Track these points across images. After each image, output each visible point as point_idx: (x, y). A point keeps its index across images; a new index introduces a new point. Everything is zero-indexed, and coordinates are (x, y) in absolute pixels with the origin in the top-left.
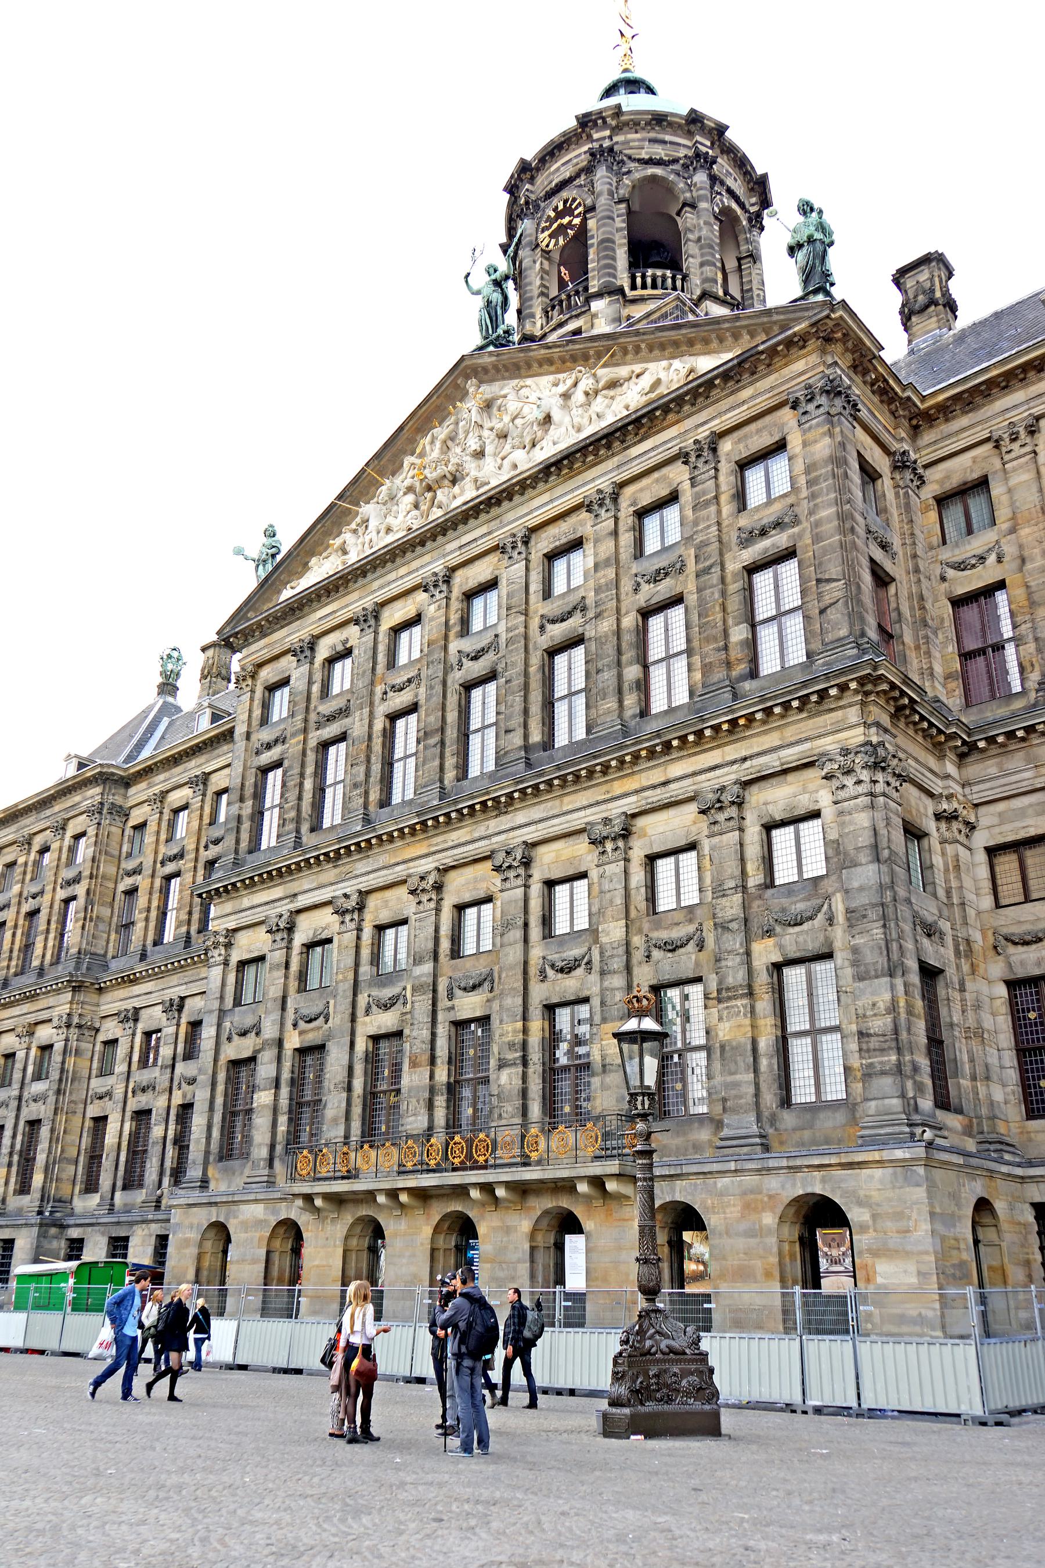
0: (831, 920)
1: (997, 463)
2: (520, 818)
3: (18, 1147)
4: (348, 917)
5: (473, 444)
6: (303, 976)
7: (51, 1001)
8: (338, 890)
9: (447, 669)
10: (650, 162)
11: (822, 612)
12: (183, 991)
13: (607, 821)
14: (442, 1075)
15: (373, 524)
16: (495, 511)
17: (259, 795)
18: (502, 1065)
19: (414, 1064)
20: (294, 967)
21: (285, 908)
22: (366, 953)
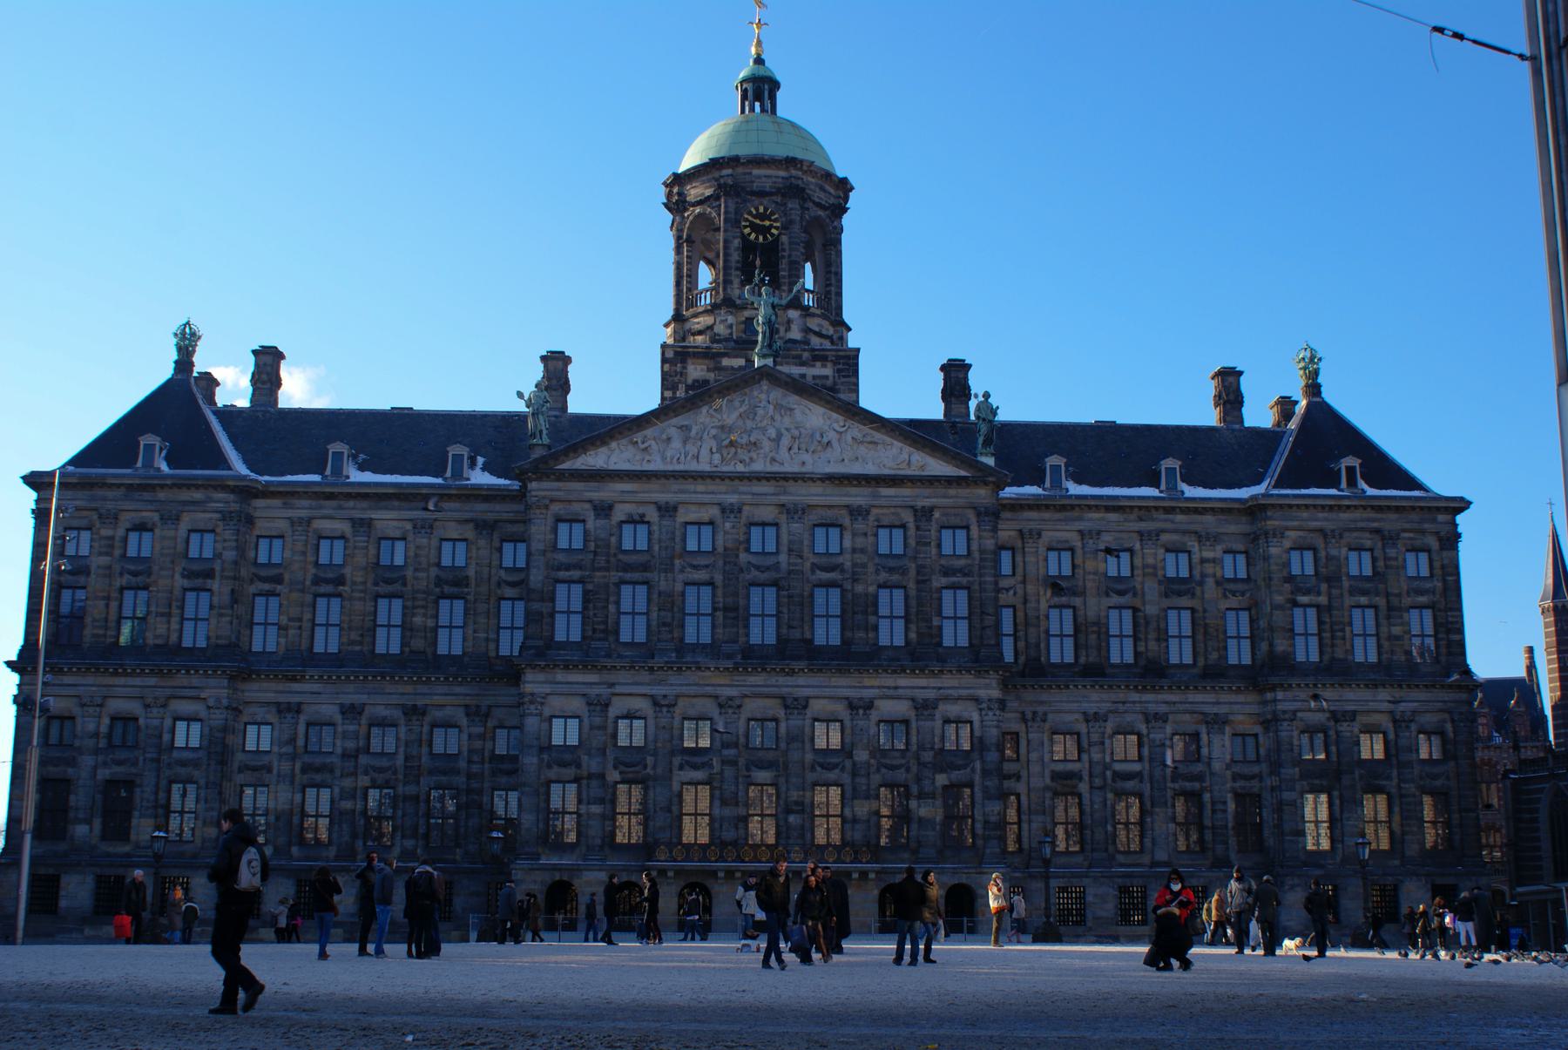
0: (973, 770)
1: (1019, 544)
2: (801, 681)
6: (615, 736)
7: (195, 681)
8: (658, 691)
9: (742, 570)
10: (819, 205)
12: (363, 698)
15: (676, 444)
16: (782, 483)
17: (553, 600)
18: (788, 811)
19: (724, 803)
20: (610, 730)
21: (603, 691)
22: (676, 732)
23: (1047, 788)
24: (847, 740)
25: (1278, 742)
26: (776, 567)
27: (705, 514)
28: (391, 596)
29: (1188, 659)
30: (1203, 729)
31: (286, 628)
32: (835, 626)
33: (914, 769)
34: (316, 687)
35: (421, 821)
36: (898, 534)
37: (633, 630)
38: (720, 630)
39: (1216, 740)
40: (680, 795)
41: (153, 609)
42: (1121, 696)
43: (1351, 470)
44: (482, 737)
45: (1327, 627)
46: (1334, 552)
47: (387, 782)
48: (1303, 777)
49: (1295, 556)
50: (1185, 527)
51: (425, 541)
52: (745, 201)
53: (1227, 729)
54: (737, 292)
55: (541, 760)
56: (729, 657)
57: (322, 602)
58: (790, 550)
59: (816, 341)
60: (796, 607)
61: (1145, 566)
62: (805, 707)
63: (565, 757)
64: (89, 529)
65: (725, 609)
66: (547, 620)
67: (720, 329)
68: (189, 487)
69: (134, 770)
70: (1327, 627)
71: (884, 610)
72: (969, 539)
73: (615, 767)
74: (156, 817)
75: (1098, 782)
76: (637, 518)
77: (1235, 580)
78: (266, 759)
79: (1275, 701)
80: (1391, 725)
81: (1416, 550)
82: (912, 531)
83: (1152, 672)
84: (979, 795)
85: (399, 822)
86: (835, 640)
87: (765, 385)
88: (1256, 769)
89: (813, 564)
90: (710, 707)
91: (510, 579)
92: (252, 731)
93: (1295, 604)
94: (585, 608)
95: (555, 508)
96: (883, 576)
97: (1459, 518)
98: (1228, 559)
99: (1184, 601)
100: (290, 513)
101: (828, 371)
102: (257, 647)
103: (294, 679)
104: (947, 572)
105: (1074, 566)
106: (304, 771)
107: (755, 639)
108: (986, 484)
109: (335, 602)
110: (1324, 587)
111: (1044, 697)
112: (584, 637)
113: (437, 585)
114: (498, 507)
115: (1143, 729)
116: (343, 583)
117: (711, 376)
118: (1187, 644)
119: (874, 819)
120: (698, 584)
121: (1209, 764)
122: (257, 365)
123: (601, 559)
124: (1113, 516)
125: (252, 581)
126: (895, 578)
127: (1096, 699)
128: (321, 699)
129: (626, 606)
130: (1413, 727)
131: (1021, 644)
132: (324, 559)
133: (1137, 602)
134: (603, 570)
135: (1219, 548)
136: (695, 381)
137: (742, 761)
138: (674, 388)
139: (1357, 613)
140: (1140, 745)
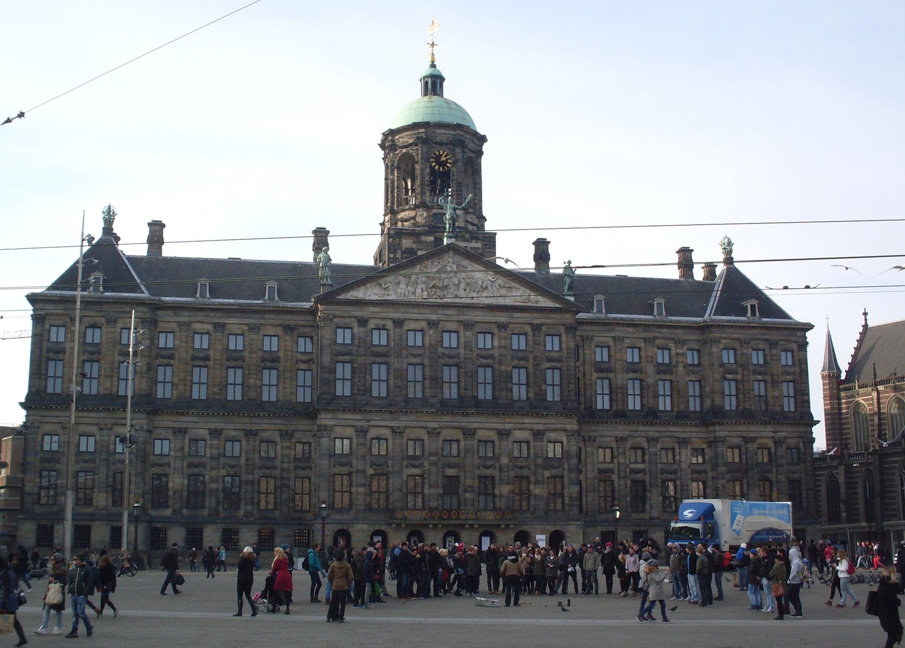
0: (564, 469)
2: (472, 419)
3: (111, 483)
5: (455, 281)
8: (395, 424)
10: (472, 151)
12: (219, 426)
14: (441, 491)
15: (403, 286)
16: (461, 309)
17: (335, 372)
18: (466, 491)
19: (431, 486)
20: (368, 445)
21: (364, 424)
22: (405, 447)
23: (596, 478)
24: (497, 451)
25: (716, 453)
27: (417, 325)
28: (235, 367)
29: (668, 408)
30: (677, 446)
31: (177, 385)
32: (489, 388)
33: (533, 467)
35: (256, 495)
36: (523, 338)
37: (379, 390)
38: (428, 391)
39: (683, 452)
40: (407, 482)
41: (102, 373)
42: (634, 428)
43: (753, 307)
44: (289, 448)
45: (741, 391)
46: (745, 351)
47: (236, 473)
48: (729, 471)
49: (725, 352)
50: (668, 336)
51: (255, 336)
52: (432, 147)
53: (689, 446)
54: (428, 199)
55: (330, 462)
56: (432, 406)
57: (196, 370)
59: (470, 227)
60: (469, 378)
61: (647, 357)
62: (474, 434)
63: (343, 460)
64: (64, 326)
65: (431, 379)
67: (419, 220)
68: (122, 303)
69: (93, 465)
70: (741, 391)
71: (515, 380)
72: (560, 342)
74: (107, 492)
75: (622, 474)
77: (693, 365)
78: (166, 459)
79: (715, 431)
80: (772, 445)
81: (785, 351)
82: (530, 337)
83: (650, 415)
84: (566, 483)
85: (243, 495)
86: (489, 396)
87: (451, 253)
88: (703, 468)
89: (478, 355)
90: (423, 434)
91: (304, 358)
92: (158, 443)
93: (726, 379)
94: (353, 377)
95: (336, 320)
96: (515, 362)
97: (808, 334)
98: (689, 353)
99: (668, 377)
100: (178, 319)
101: (479, 245)
102: (160, 395)
103: (183, 414)
104: (549, 360)
105: (609, 356)
106: (189, 466)
107: (446, 396)
108: (570, 311)
109: (204, 370)
110: (740, 370)
111: (594, 428)
112: (352, 394)
114: (296, 317)
115: (645, 445)
116: (209, 360)
117: (415, 246)
118: (668, 400)
119: (511, 495)
120: (414, 365)
121: (680, 465)
122: (151, 232)
123: (362, 350)
124: (630, 329)
125: (157, 358)
126: (522, 363)
127: (621, 430)
128: (199, 427)
129: (375, 376)
130: (784, 445)
131: (582, 399)
132: (197, 345)
133: (642, 377)
134: (362, 356)
135: (685, 347)
137: (440, 464)
138: (395, 253)
139: (756, 384)
140: (644, 454)
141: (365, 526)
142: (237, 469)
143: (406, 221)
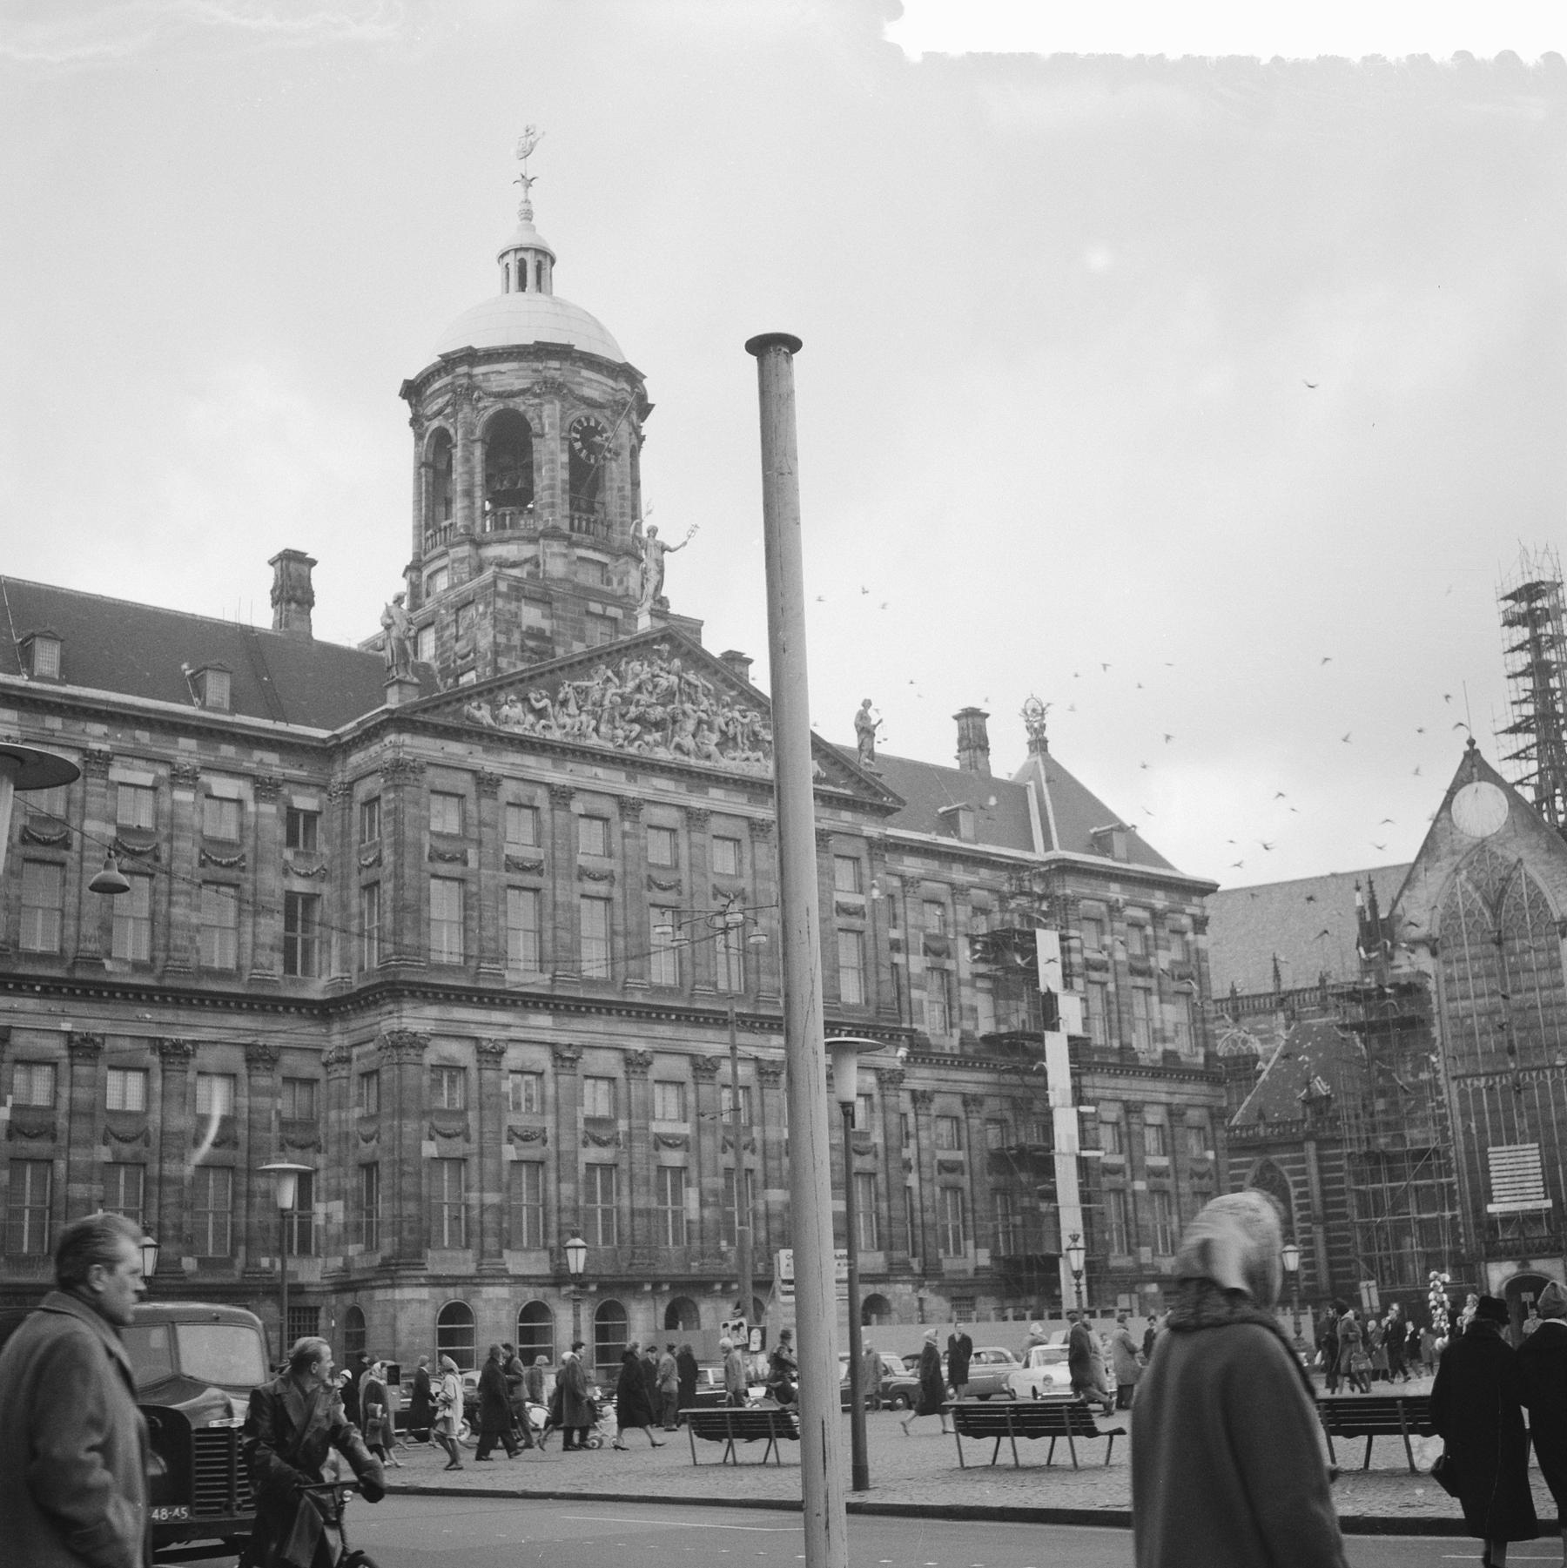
0: (876, 1156)
4: (568, 1064)
8: (564, 1039)
11: (879, 983)
12: (101, 1027)
13: (773, 1062)
15: (572, 709)
26: (676, 887)
34: (31, 1004)
42: (943, 1074)
47: (136, 1155)
51: (184, 796)
52: (573, 407)
58: (691, 865)
61: (956, 924)
65: (627, 934)
66: (423, 928)
70: (1114, 1007)
73: (510, 1141)
76: (525, 801)
95: (431, 772)
113: (202, 864)
117: (546, 625)
136: (529, 627)
138: (508, 633)
141: (502, 1292)
142: (137, 1146)
143: (514, 565)
